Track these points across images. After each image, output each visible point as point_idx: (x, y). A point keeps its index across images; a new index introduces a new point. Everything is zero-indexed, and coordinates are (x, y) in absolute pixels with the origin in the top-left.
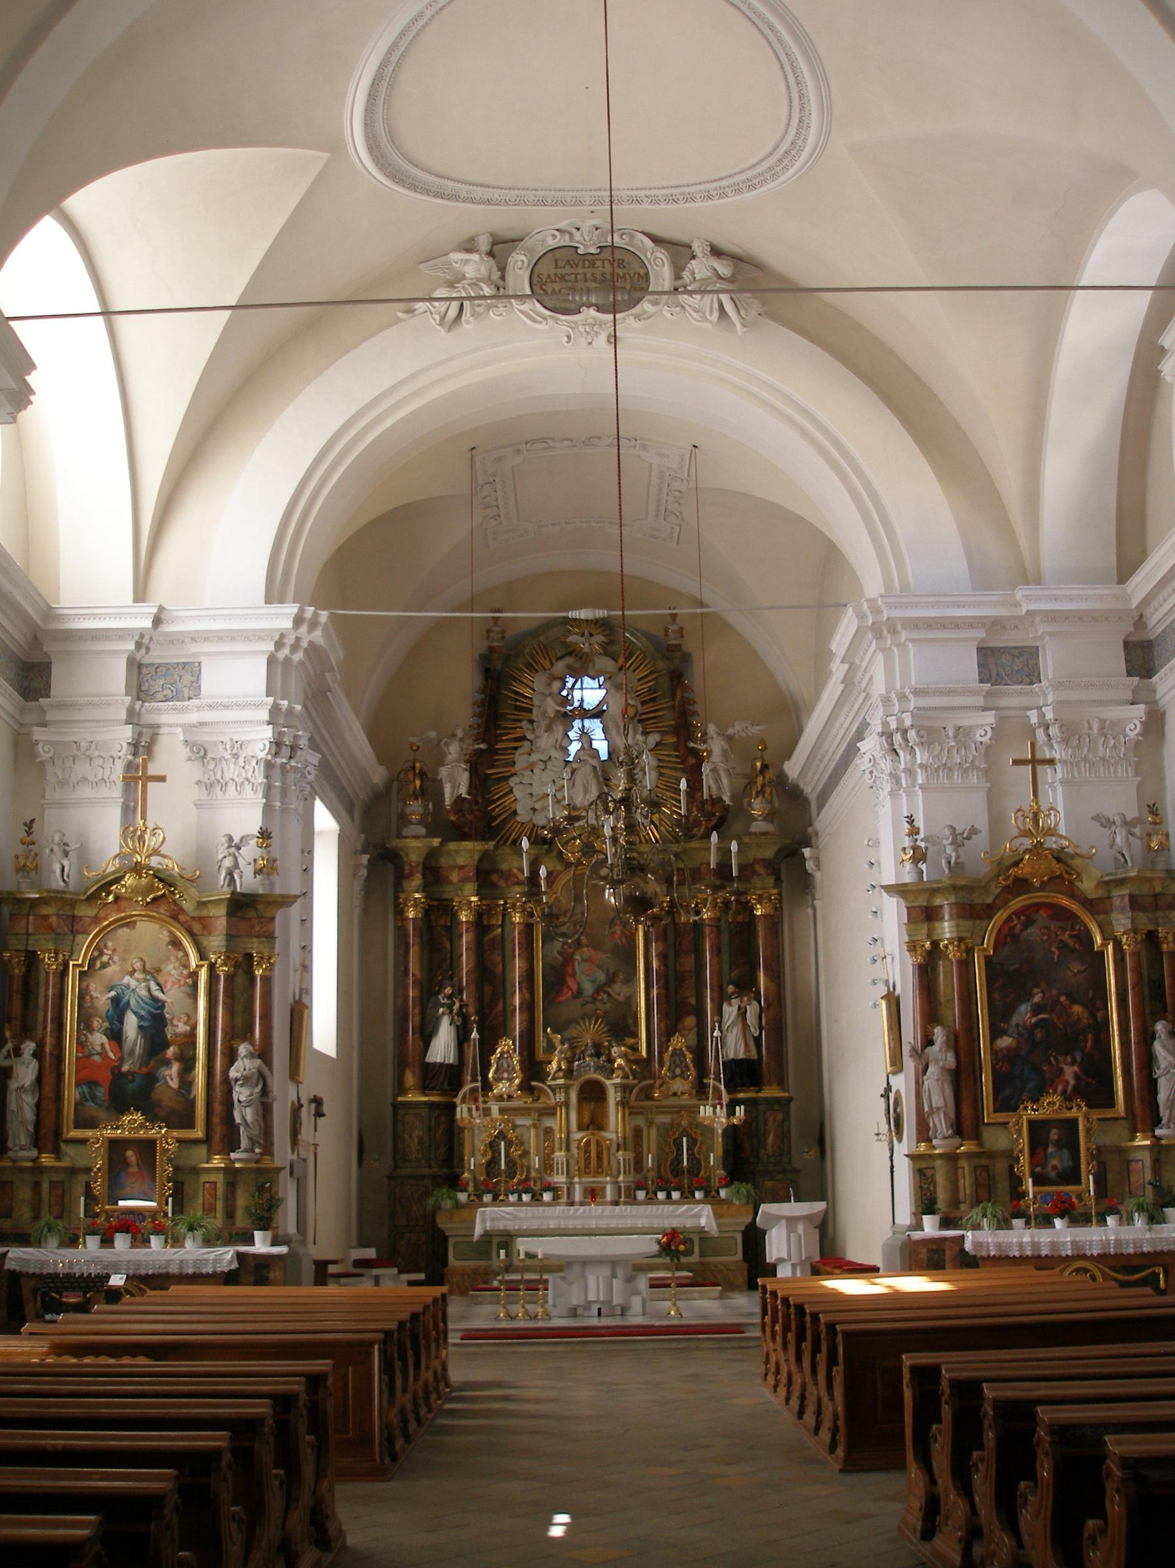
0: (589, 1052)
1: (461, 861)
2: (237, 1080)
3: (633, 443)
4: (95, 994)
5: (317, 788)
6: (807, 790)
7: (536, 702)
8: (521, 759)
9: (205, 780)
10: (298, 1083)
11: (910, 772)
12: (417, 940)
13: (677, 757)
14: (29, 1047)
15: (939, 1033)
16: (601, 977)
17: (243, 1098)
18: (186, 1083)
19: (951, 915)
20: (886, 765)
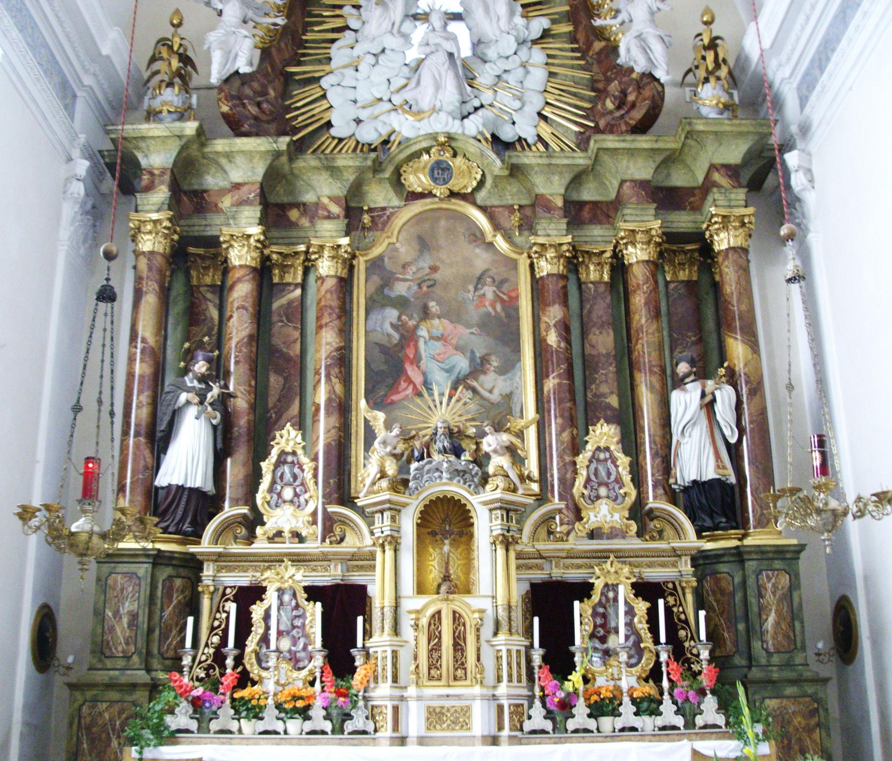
0: (439, 445)
1: (236, 176)
8: (339, 53)
13: (573, 50)
16: (462, 364)
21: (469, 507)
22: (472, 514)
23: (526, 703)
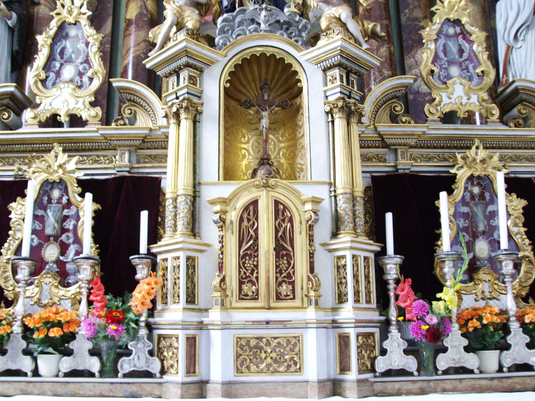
21: (296, 67)
22: (301, 76)
23: (377, 331)
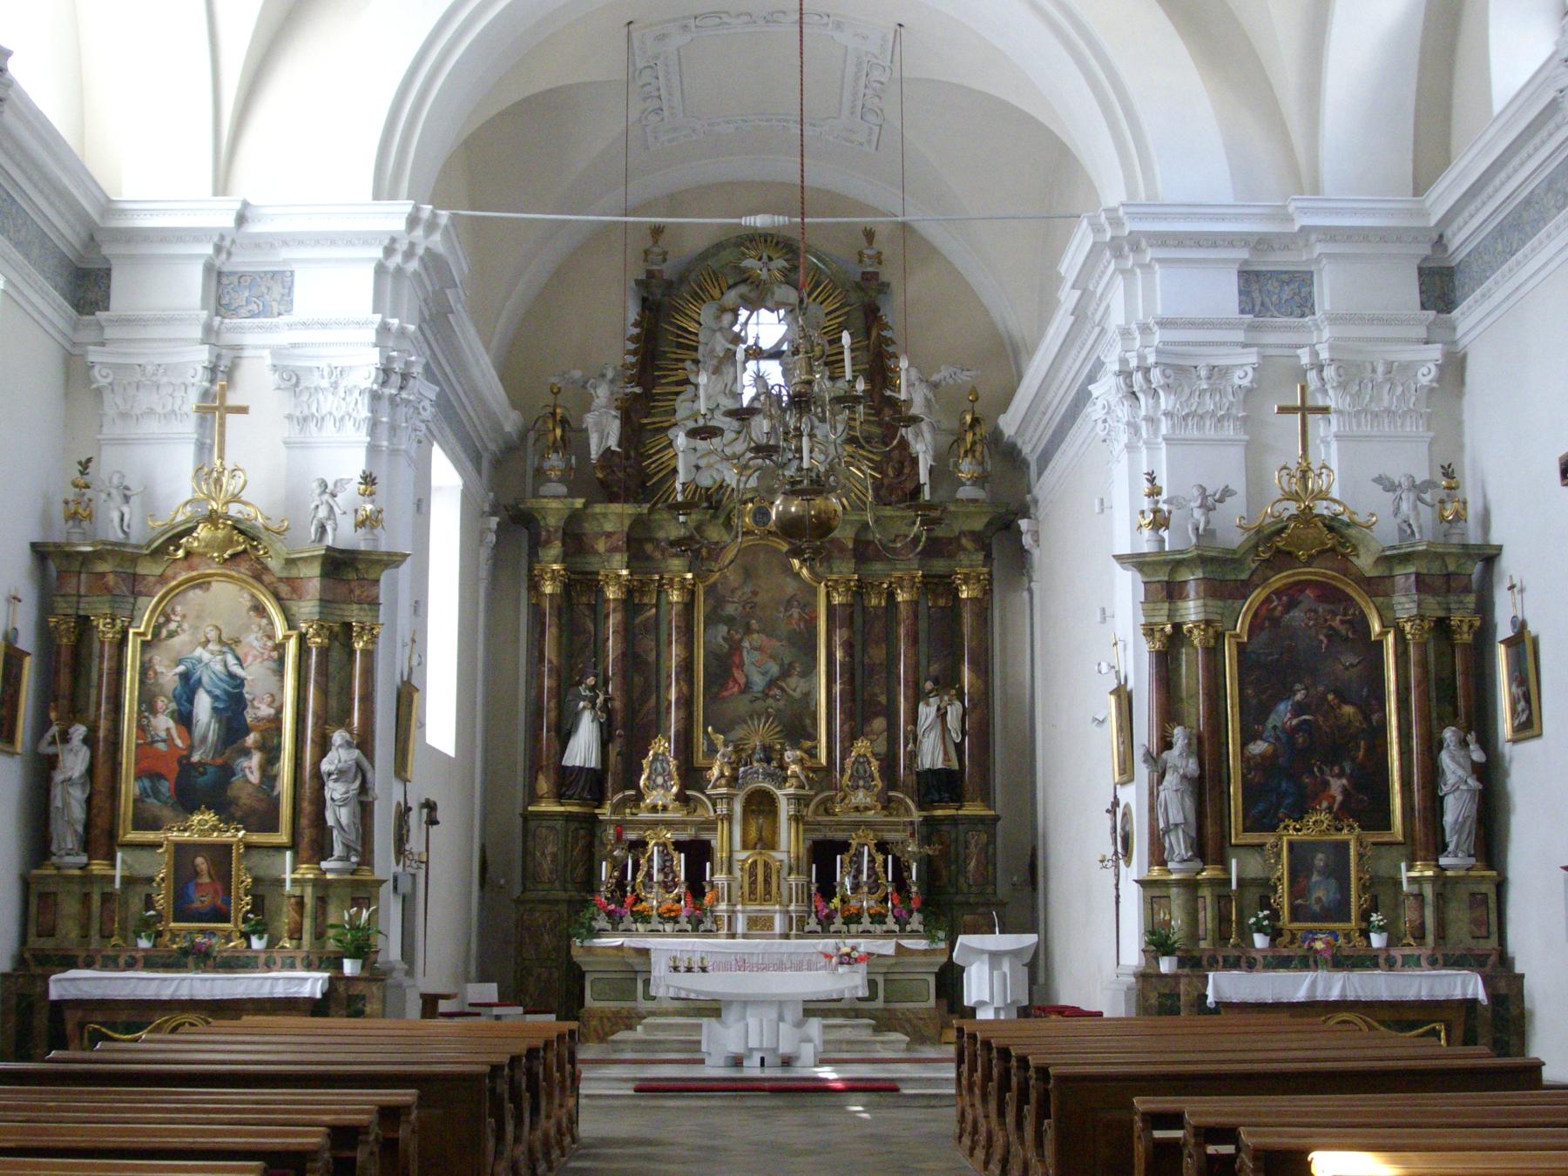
1: (609, 527)
2: (330, 774)
3: (825, 19)
4: (159, 669)
5: (436, 432)
6: (1026, 450)
7: (702, 338)
9: (298, 413)
10: (405, 781)
11: (1152, 420)
12: (555, 620)
14: (79, 731)
15: (1178, 733)
16: (775, 669)
17: (337, 796)
18: (269, 776)
19: (1197, 593)
20: (1123, 411)
